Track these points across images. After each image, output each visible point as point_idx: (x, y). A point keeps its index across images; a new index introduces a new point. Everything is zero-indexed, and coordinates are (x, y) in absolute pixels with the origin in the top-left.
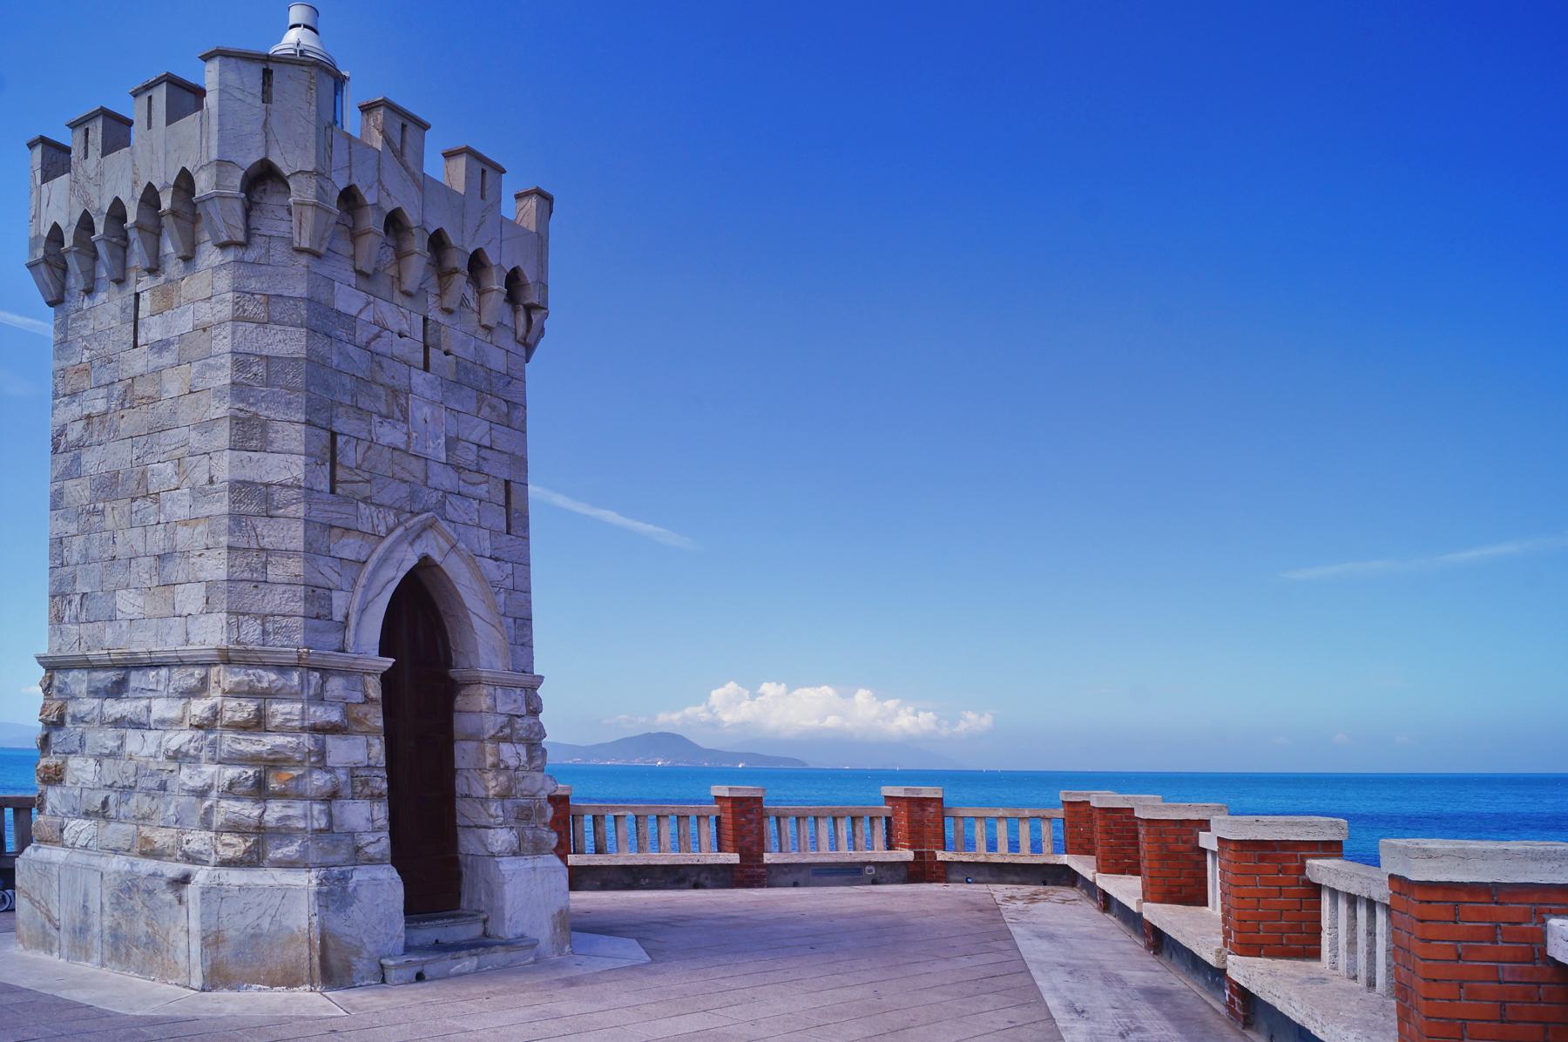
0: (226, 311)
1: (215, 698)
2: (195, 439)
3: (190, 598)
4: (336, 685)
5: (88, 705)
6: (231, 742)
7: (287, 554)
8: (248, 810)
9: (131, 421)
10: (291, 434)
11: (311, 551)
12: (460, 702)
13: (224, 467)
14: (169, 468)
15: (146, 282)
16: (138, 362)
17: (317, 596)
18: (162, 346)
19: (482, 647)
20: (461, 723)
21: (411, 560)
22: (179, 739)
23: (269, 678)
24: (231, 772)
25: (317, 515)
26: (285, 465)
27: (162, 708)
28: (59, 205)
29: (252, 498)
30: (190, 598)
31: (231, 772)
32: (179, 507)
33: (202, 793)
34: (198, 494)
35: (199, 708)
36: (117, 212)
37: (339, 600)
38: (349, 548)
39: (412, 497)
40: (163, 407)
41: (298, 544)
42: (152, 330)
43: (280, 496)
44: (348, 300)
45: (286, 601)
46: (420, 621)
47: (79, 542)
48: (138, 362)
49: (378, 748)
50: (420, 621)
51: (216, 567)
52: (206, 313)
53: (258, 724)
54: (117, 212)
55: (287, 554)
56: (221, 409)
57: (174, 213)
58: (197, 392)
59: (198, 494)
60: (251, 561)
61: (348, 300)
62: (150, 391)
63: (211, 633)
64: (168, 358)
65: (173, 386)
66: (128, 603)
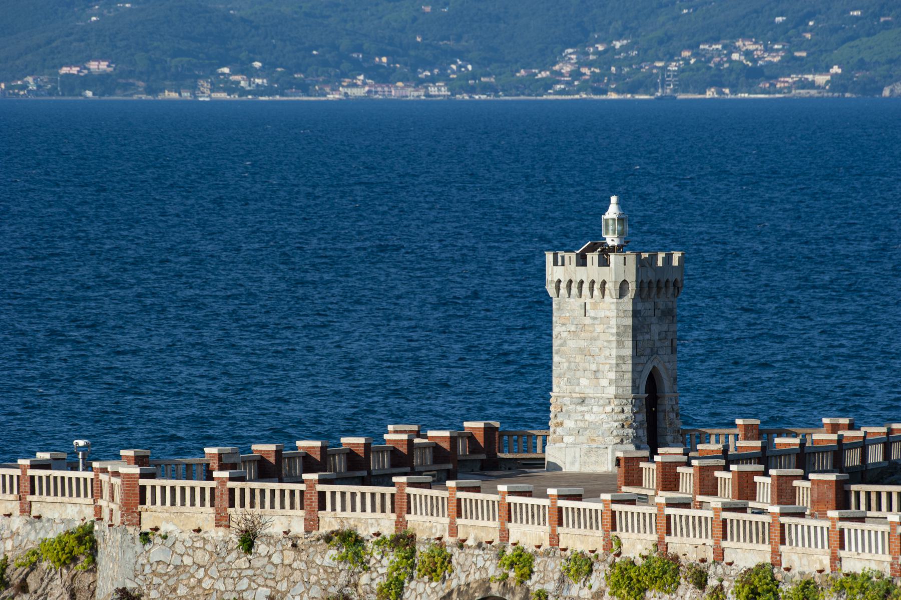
0: (614, 314)
2: (605, 344)
3: (604, 382)
7: (628, 372)
12: (659, 401)
14: (597, 350)
15: (589, 301)
16: (587, 321)
18: (595, 318)
24: (616, 424)
26: (628, 351)
30: (604, 382)
33: (609, 429)
41: (630, 369)
42: (591, 313)
48: (587, 321)
51: (612, 375)
52: (608, 313)
55: (628, 372)
62: (591, 329)
64: (596, 322)
65: (599, 328)
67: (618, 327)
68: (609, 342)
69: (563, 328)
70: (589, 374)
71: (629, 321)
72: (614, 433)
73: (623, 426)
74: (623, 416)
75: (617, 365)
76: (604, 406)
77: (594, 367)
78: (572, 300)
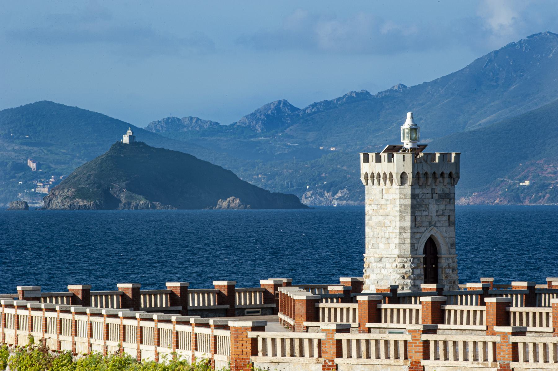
2: (393, 218)
3: (392, 246)
7: (407, 238)
9: (381, 212)
14: (389, 223)
15: (384, 187)
16: (383, 202)
18: (387, 200)
24: (399, 276)
25: (414, 231)
29: (402, 228)
31: (399, 276)
32: (390, 229)
35: (394, 265)
42: (385, 196)
47: (372, 233)
48: (383, 202)
51: (397, 241)
54: (379, 175)
55: (407, 238)
59: (394, 228)
64: (388, 202)
65: (390, 207)
66: (382, 246)
68: (395, 216)
70: (384, 240)
75: (400, 233)
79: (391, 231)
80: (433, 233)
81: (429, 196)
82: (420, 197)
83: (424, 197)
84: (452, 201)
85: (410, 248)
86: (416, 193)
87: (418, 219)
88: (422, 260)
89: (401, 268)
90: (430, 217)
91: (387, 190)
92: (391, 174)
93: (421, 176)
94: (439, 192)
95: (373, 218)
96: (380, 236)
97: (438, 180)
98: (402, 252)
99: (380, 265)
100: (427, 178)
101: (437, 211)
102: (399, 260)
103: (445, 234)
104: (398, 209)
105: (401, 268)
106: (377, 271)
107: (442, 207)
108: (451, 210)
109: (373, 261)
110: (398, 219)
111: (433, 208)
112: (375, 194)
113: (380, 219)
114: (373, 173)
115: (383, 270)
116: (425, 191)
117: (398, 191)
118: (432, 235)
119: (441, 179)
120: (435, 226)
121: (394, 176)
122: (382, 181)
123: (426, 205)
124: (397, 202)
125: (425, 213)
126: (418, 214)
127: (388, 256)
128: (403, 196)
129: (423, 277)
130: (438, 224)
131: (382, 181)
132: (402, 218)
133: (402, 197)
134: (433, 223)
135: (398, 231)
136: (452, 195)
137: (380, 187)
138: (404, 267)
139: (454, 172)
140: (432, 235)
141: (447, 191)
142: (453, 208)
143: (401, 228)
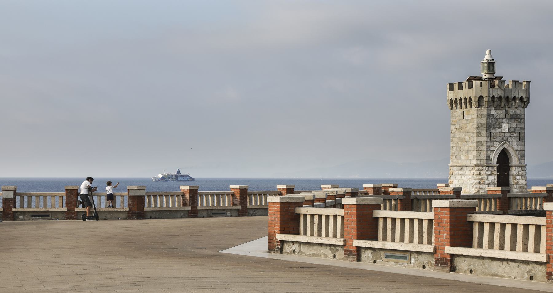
0: (476, 116)
1: (474, 171)
2: (472, 135)
3: (471, 157)
4: (490, 169)
5: (457, 172)
6: (475, 177)
7: (484, 151)
8: (478, 186)
9: (462, 130)
10: (484, 134)
11: (487, 150)
13: (476, 139)
14: (468, 138)
15: (465, 110)
16: (464, 122)
17: (488, 157)
18: (467, 120)
19: (514, 160)
20: (511, 173)
21: (502, 148)
22: (470, 177)
23: (481, 168)
24: (476, 181)
25: (488, 145)
26: (484, 138)
27: (467, 172)
28: (451, 95)
29: (479, 143)
30: (471, 157)
31: (476, 181)
32: (469, 144)
34: (472, 143)
35: (472, 173)
36: (461, 99)
37: (491, 156)
38: (492, 149)
39: (502, 139)
40: (468, 129)
42: (466, 117)
43: (483, 143)
44: (493, 112)
45: (483, 157)
46: (504, 159)
47: (455, 148)
48: (464, 122)
49: (496, 177)
50: (504, 159)
51: (474, 153)
53: (480, 174)
54: (461, 99)
55: (484, 151)
56: (475, 131)
57: (468, 101)
58: (472, 128)
59: (472, 143)
60: (479, 151)
61: (493, 112)
63: (474, 162)
64: (468, 122)
65: (469, 126)
66: (462, 157)
67: (478, 124)
68: (473, 133)
69: (454, 127)
70: (464, 153)
71: (484, 121)
72: (474, 187)
73: (480, 183)
74: (480, 177)
75: (477, 146)
76: (471, 170)
77: (467, 149)
78: (458, 110)
79: (470, 145)
80: (505, 146)
81: (502, 116)
82: (495, 117)
83: (498, 117)
84: (522, 120)
85: (485, 158)
86: (491, 113)
87: (493, 135)
88: (495, 168)
89: (478, 175)
90: (503, 134)
91: (468, 112)
92: (470, 98)
93: (496, 100)
94: (511, 113)
95: (456, 135)
96: (461, 149)
97: (510, 103)
98: (479, 161)
99: (461, 172)
100: (501, 102)
101: (509, 129)
102: (476, 168)
103: (516, 148)
104: (475, 126)
105: (478, 175)
106: (459, 177)
107: (514, 125)
108: (521, 128)
109: (455, 170)
110: (475, 134)
111: (505, 127)
112: (458, 116)
113: (461, 135)
114: (456, 99)
115: (463, 176)
116: (499, 112)
117: (476, 112)
118: (504, 148)
119: (513, 102)
120: (507, 141)
121: (473, 100)
122: (463, 105)
123: (500, 123)
124: (475, 122)
125: (499, 130)
126: (492, 131)
127: (467, 165)
128: (480, 116)
129: (496, 182)
130: (510, 140)
131: (463, 105)
132: (479, 134)
133: (480, 116)
134: (506, 138)
135: (475, 145)
136: (523, 116)
137: (462, 110)
138: (480, 174)
139: (524, 97)
140: (504, 148)
141: (518, 112)
142: (523, 126)
143: (478, 142)
